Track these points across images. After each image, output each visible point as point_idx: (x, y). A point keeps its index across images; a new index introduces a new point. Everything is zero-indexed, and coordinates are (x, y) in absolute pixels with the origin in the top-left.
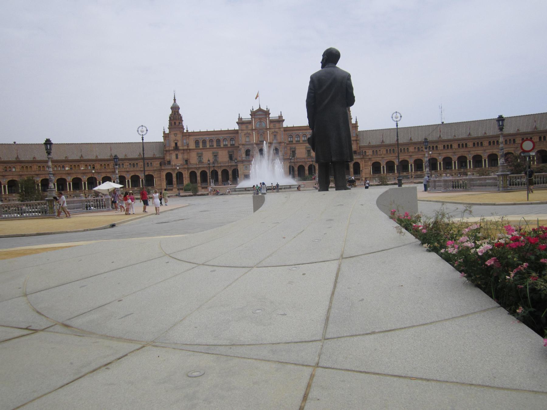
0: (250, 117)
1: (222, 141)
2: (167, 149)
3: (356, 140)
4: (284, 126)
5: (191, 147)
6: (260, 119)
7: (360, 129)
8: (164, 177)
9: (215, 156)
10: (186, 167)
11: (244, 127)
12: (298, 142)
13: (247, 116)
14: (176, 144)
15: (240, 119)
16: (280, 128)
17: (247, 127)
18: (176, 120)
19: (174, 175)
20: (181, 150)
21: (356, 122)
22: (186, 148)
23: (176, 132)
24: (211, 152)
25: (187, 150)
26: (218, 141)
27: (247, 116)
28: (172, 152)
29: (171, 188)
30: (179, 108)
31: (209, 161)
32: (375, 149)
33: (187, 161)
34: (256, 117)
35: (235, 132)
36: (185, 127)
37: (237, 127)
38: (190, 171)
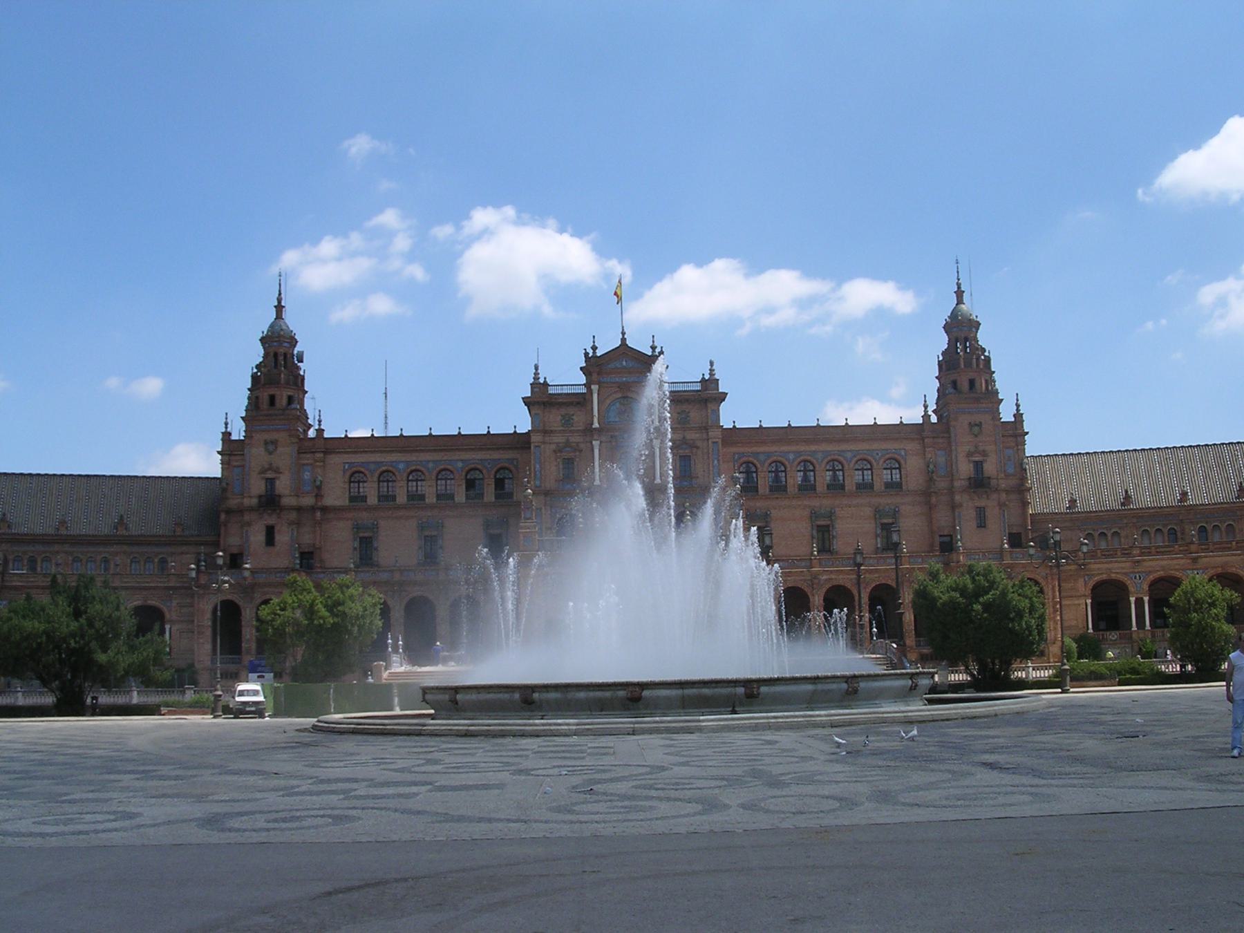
0: (582, 379)
2: (233, 502)
4: (726, 423)
5: (329, 501)
7: (1032, 447)
8: (207, 622)
11: (554, 418)
13: (567, 375)
14: (271, 482)
15: (539, 387)
17: (567, 421)
21: (1018, 416)
22: (308, 501)
23: (275, 436)
25: (313, 509)
27: (567, 375)
30: (293, 342)
35: (518, 442)
37: (522, 422)
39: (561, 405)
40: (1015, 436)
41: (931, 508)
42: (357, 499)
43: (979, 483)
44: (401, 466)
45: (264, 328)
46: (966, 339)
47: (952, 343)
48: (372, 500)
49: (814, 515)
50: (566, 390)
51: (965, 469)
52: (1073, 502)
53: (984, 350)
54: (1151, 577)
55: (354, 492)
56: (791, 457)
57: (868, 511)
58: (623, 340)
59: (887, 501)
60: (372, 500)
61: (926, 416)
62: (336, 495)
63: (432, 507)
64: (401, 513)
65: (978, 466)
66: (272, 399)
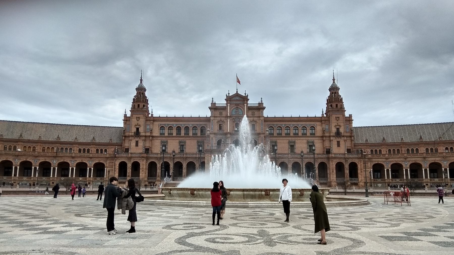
0: (225, 102)
1: (191, 129)
2: (127, 134)
3: (351, 137)
4: (265, 115)
6: (237, 105)
9: (182, 146)
10: (145, 155)
11: (217, 113)
12: (280, 135)
14: (138, 129)
15: (213, 104)
16: (259, 117)
17: (221, 114)
18: (140, 102)
19: (129, 165)
20: (143, 136)
21: (351, 116)
22: (148, 134)
24: (178, 141)
25: (149, 136)
26: (187, 128)
28: (132, 138)
29: (124, 180)
30: (145, 90)
31: (174, 152)
32: (376, 148)
33: (147, 150)
34: (232, 102)
35: (207, 119)
36: (150, 112)
37: (208, 114)
38: (149, 162)
39: (219, 109)
40: (349, 121)
41: (324, 141)
42: (162, 134)
43: (338, 134)
44: (175, 125)
45: (137, 86)
46: (335, 93)
47: (331, 94)
48: (166, 134)
49: (289, 142)
50: (221, 105)
51: (334, 130)
52: (367, 140)
53: (340, 96)
54: (392, 163)
55: (161, 132)
56: (283, 125)
57: (305, 141)
58: (237, 92)
59: (311, 139)
60: (166, 134)
61: (323, 115)
62: (156, 133)
63: (183, 137)
64: (174, 138)
65: (338, 129)
66: (139, 105)
